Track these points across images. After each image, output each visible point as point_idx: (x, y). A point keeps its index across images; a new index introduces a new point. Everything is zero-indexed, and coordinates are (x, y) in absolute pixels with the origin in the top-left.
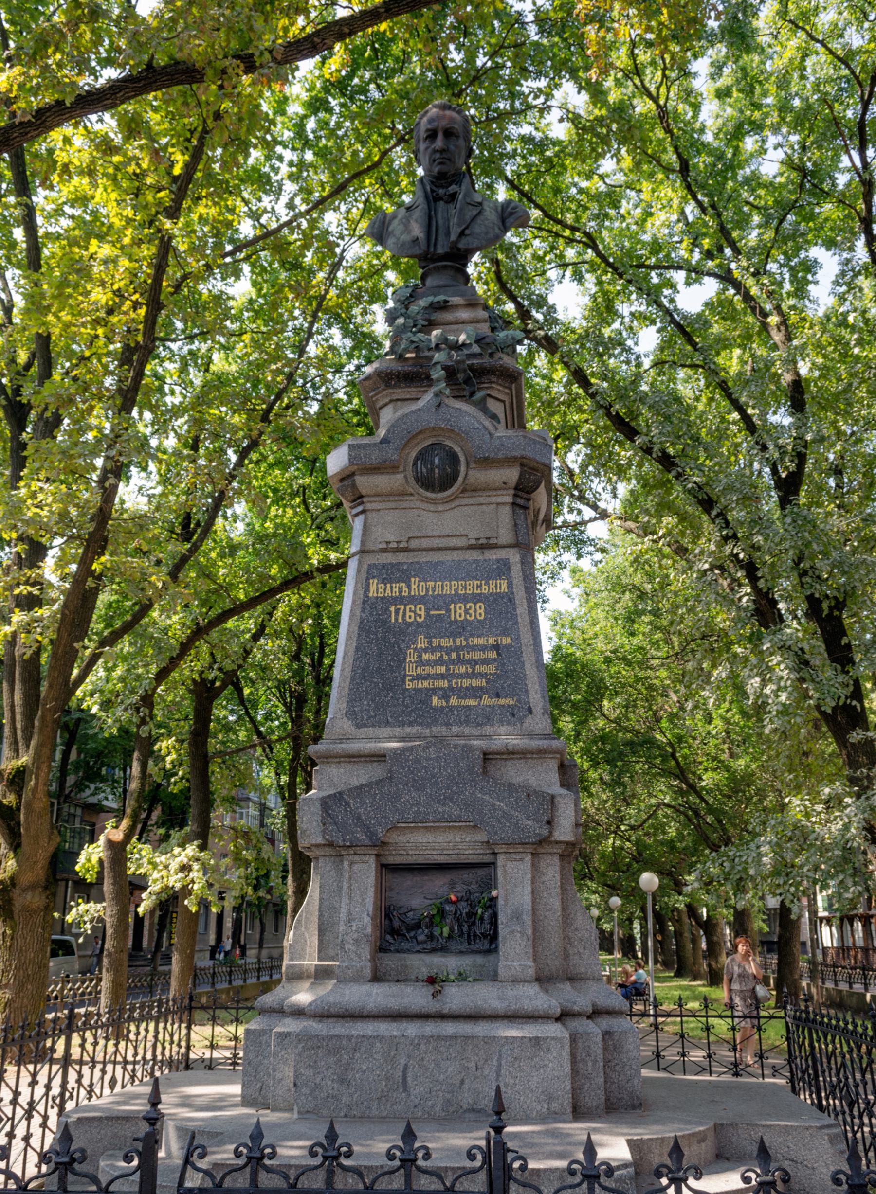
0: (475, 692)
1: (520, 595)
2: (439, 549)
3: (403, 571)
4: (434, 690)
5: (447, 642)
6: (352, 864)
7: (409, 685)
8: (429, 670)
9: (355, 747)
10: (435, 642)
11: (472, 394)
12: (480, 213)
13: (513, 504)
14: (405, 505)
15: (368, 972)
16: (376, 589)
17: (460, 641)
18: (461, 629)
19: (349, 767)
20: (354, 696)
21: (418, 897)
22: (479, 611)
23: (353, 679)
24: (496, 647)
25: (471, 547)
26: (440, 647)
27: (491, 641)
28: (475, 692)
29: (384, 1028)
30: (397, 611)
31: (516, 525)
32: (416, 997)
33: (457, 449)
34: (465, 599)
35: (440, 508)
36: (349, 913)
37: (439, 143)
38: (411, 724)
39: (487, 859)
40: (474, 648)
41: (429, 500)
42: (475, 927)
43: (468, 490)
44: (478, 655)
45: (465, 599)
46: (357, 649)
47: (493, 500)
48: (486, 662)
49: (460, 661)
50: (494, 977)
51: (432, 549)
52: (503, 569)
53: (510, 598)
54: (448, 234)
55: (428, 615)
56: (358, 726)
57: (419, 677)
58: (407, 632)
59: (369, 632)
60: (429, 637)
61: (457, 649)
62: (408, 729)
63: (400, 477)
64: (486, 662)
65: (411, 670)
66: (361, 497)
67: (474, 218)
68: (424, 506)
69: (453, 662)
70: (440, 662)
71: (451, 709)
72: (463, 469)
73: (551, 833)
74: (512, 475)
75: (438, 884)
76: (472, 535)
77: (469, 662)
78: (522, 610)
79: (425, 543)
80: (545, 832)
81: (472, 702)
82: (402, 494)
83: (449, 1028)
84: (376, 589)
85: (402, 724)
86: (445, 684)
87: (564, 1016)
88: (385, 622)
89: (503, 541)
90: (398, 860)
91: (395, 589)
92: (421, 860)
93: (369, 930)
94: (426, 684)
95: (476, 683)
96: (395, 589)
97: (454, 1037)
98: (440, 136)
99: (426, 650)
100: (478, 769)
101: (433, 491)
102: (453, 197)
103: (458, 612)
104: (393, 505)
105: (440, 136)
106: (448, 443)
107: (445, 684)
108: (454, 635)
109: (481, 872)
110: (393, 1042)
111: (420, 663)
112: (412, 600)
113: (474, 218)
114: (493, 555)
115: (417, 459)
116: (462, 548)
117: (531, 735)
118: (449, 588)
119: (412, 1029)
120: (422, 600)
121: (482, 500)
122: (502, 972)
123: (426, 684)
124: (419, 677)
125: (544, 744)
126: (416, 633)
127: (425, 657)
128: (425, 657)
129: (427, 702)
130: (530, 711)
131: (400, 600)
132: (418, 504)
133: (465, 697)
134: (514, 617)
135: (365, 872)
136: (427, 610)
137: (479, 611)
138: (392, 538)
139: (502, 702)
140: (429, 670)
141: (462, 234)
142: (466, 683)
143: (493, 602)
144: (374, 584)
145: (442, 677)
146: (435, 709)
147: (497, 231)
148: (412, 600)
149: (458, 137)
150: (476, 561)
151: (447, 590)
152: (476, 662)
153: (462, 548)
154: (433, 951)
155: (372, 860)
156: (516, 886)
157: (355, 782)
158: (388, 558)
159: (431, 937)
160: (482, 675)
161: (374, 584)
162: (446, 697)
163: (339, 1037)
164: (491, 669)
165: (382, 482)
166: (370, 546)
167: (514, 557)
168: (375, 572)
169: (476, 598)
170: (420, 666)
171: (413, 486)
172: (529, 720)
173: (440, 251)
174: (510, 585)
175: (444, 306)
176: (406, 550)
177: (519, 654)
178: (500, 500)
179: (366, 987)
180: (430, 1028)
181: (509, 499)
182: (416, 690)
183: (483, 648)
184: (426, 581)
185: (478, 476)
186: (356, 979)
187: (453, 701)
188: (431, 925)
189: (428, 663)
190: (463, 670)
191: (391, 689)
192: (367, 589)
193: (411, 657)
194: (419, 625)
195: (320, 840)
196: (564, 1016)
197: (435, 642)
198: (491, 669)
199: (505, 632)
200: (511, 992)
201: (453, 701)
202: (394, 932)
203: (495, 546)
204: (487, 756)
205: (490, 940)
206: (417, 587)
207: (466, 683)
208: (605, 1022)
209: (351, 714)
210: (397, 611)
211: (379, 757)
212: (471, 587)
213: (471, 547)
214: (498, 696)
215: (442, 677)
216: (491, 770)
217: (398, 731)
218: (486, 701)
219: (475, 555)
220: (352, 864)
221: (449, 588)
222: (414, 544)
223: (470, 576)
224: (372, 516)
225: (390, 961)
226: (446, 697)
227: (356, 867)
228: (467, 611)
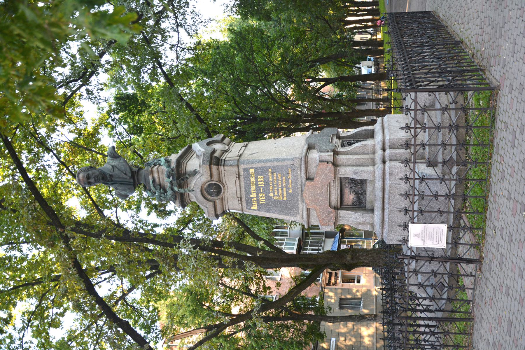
0: (287, 180)
1: (255, 165)
2: (240, 188)
3: (248, 199)
4: (287, 192)
5: (271, 188)
6: (340, 217)
7: (285, 199)
8: (280, 193)
10: (271, 191)
11: (187, 178)
12: (116, 167)
13: (224, 166)
14: (226, 199)
15: (371, 215)
16: (254, 207)
17: (271, 184)
18: (266, 182)
19: (311, 217)
21: (350, 197)
23: (284, 215)
24: (272, 173)
25: (239, 179)
26: (273, 190)
27: (270, 175)
28: (287, 180)
29: (386, 213)
30: (261, 201)
31: (231, 165)
32: (378, 205)
33: (207, 184)
34: (257, 182)
35: (226, 188)
36: (355, 218)
37: (92, 180)
38: (298, 199)
39: (339, 179)
40: (273, 180)
41: (224, 192)
42: (359, 185)
44: (275, 179)
45: (257, 182)
46: (274, 213)
47: (223, 172)
48: (277, 177)
49: (277, 184)
51: (240, 190)
52: (246, 170)
53: (256, 168)
54: (125, 178)
55: (262, 193)
56: (299, 213)
57: (283, 196)
58: (268, 199)
59: (269, 210)
60: (270, 193)
61: (273, 184)
62: (299, 200)
63: (217, 201)
64: (277, 177)
65: (280, 198)
66: (224, 211)
67: (119, 170)
68: (226, 192)
69: (277, 186)
70: (278, 190)
71: (292, 187)
72: (213, 182)
73: (331, 162)
74: (214, 168)
75: (347, 191)
76: (235, 179)
77: (277, 181)
78: (260, 165)
79: (239, 192)
80: (330, 165)
81: (290, 181)
82: (222, 199)
83: (386, 196)
84: (254, 207)
85: (298, 201)
86: (285, 189)
87: (384, 162)
88: (265, 205)
89: (236, 169)
90: (339, 203)
91: (254, 202)
92: (339, 197)
93: (359, 214)
94: (285, 194)
95: (284, 180)
96: (254, 202)
97: (389, 196)
98: (90, 180)
99: (274, 194)
100: (312, 183)
101: (221, 190)
102: (110, 175)
103: (261, 184)
104: (226, 202)
105: (90, 180)
106: (205, 187)
107: (285, 189)
108: (269, 185)
109: (342, 180)
110: (390, 211)
111: (278, 195)
112: (258, 197)
113: (119, 170)
114: (242, 173)
115: (211, 196)
116: (240, 182)
117: (301, 165)
118: (253, 186)
119: (387, 206)
120: (258, 194)
121: (223, 176)
122: (371, 179)
123: (285, 194)
124: (283, 196)
125: (303, 163)
126: (269, 197)
127: (276, 194)
128: (276, 194)
129: (290, 194)
130: (293, 164)
131: (258, 200)
132: (225, 194)
133: (289, 183)
134: (263, 167)
135: (342, 213)
136: (261, 193)
137: (261, 178)
138: (237, 202)
139: (290, 172)
140: (280, 193)
141: (125, 174)
142: (284, 182)
143: (257, 174)
144: (253, 208)
145: (282, 189)
146: (293, 192)
147: (122, 161)
148: (258, 197)
149: (88, 174)
150: (244, 178)
151: (254, 187)
152: (277, 179)
153: (240, 182)
154: (366, 194)
155: (339, 211)
156: (347, 172)
157: (316, 215)
158: (244, 203)
159: (361, 194)
160: (282, 178)
161: (253, 208)
162: (289, 188)
163: (388, 225)
164: (279, 175)
166: (240, 208)
167: (242, 167)
168: (249, 207)
169: (256, 178)
170: (280, 196)
171: (220, 197)
172: (295, 165)
173: (132, 181)
174: (252, 168)
175: (154, 181)
176: (241, 198)
177: (274, 167)
178: (223, 170)
179: (375, 216)
180: (386, 201)
181: (222, 167)
182: (287, 197)
183: (273, 177)
184: (251, 193)
185: (215, 178)
186: (373, 218)
187: (290, 186)
188: (358, 194)
189: (278, 193)
190: (280, 183)
191: (287, 204)
192: (255, 210)
193: (277, 198)
194: (266, 195)
195: (334, 226)
196: (384, 162)
197: (271, 191)
198: (279, 175)
199: (268, 171)
200: (377, 178)
201: (290, 186)
202: (360, 203)
203: (239, 172)
204: (308, 179)
205: (362, 182)
206: (253, 195)
207: (284, 182)
208: (387, 147)
209: (295, 215)
210: (261, 201)
211: (308, 210)
212: (253, 180)
213: (239, 179)
214: (288, 174)
215: (282, 189)
216: (312, 177)
217: (300, 202)
218: (290, 177)
219: (242, 178)
220: (340, 217)
221: (253, 186)
222: (239, 196)
223: (249, 180)
224: (230, 207)
225: (369, 206)
226: (289, 188)
227: (341, 216)
228: (261, 181)
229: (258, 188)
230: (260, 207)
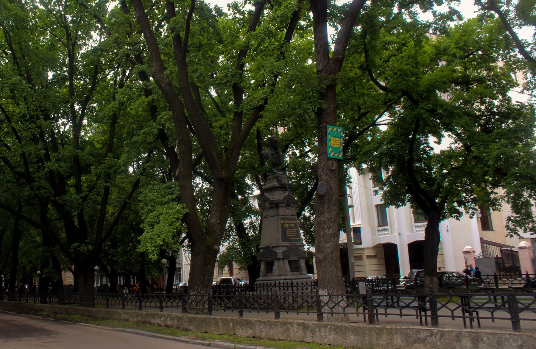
0: (294, 237)
9: (284, 244)
16: (282, 221)
18: (292, 228)
20: (282, 237)
22: (293, 225)
28: (294, 237)
43: (292, 207)
50: (301, 274)
58: (286, 228)
65: (287, 234)
84: (282, 221)
91: (283, 222)
96: (283, 222)
103: (291, 225)
118: (290, 222)
165: (282, 205)
206: (286, 221)
209: (282, 240)
212: (292, 222)
221: (290, 222)
229: (289, 224)
230: (282, 224)
